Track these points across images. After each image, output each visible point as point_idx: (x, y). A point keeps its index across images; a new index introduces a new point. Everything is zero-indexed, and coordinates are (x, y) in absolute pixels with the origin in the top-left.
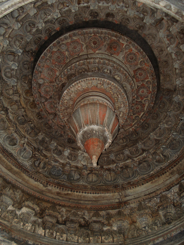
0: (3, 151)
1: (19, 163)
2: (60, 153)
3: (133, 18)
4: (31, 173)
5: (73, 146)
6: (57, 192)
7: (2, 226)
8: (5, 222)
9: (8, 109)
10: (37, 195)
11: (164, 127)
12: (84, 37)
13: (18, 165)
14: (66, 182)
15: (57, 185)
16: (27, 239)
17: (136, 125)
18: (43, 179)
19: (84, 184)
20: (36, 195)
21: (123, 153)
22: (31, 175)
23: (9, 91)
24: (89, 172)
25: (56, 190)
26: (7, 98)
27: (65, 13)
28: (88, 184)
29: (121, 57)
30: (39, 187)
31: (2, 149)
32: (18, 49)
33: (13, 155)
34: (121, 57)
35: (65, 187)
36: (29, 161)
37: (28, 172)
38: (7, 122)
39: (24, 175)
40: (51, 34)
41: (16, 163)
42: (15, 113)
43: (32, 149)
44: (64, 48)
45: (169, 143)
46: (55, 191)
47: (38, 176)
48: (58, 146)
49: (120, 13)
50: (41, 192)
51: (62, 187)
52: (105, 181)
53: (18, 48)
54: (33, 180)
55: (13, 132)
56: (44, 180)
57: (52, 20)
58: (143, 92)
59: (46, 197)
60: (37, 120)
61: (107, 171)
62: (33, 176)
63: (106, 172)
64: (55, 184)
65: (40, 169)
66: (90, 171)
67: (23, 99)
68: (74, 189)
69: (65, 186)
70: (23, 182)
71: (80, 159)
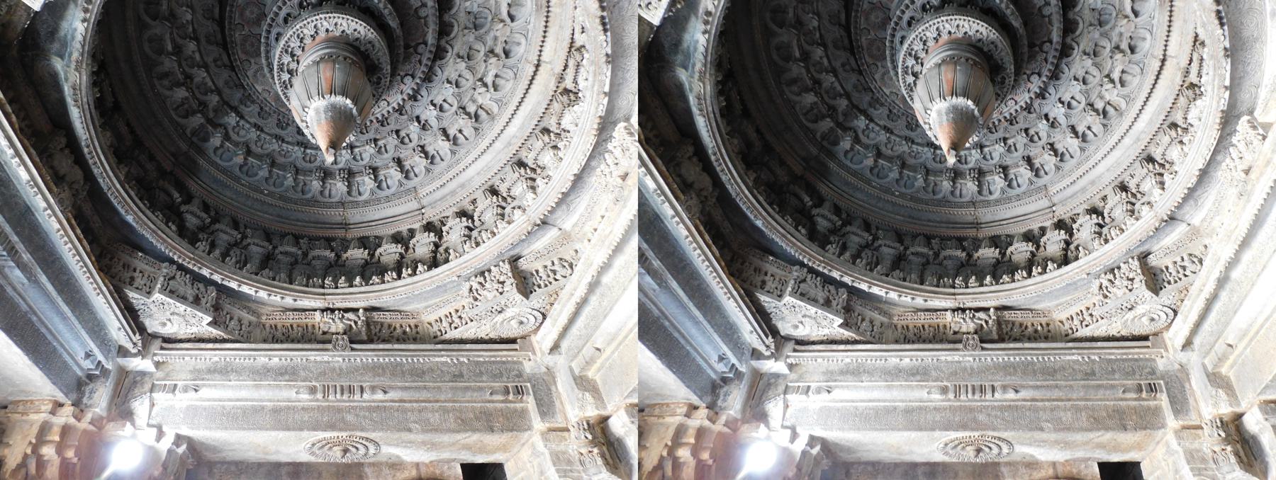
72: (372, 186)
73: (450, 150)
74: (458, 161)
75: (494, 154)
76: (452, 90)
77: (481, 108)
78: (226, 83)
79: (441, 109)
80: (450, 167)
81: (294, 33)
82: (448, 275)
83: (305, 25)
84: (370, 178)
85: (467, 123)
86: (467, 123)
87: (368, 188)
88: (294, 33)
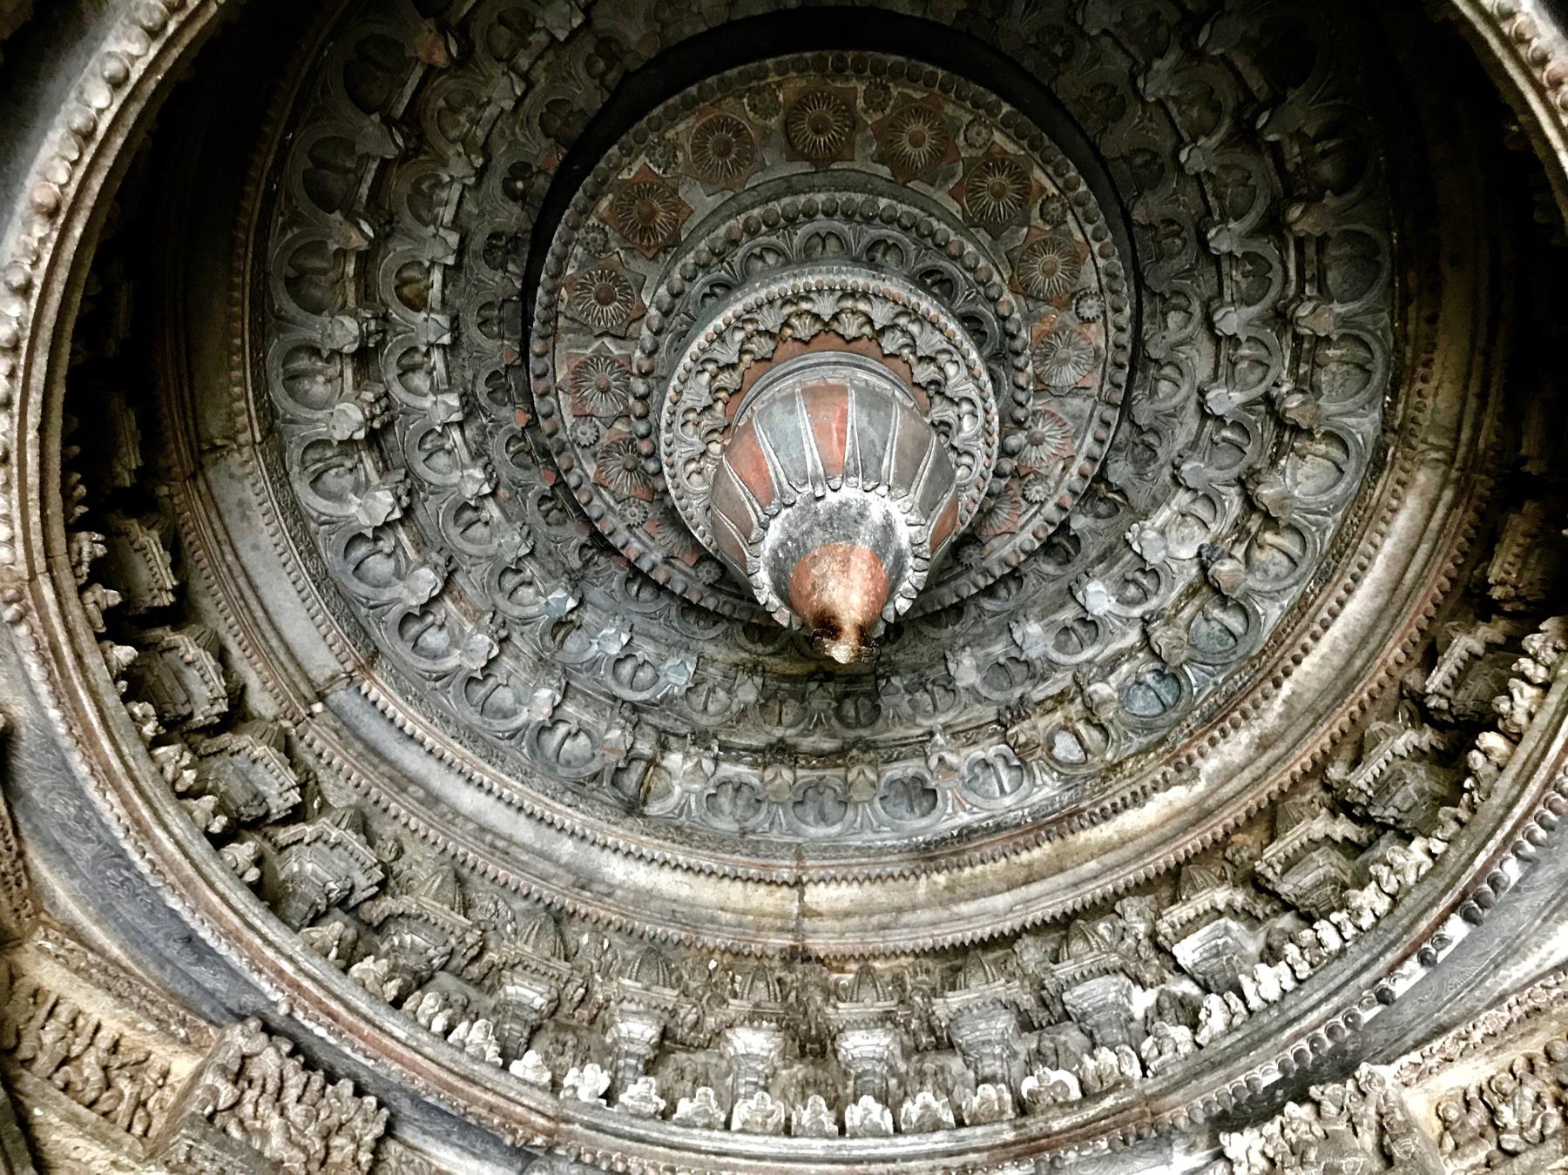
0: (924, 859)
1: (1018, 825)
2: (1090, 624)
3: (552, 82)
5: (1093, 554)
6: (1251, 742)
7: (1104, 1131)
8: (1109, 1102)
9: (781, 740)
10: (1192, 842)
12: (568, 330)
13: (1022, 834)
14: (1231, 677)
15: (1213, 727)
16: (1242, 1078)
18: (1147, 769)
19: (1285, 602)
20: (1189, 847)
21: (1234, 340)
22: (1097, 810)
24: (1239, 551)
25: (1237, 746)
26: (738, 722)
28: (1296, 583)
29: (700, 200)
30: (1178, 805)
31: (915, 854)
32: (547, 604)
33: (976, 825)
34: (700, 200)
35: (1241, 701)
36: (1039, 782)
37: (1078, 813)
38: (828, 772)
39: (1082, 836)
41: (1010, 837)
43: (995, 739)
44: (585, 433)
46: (1241, 748)
47: (1123, 784)
48: (1052, 618)
49: (514, 134)
50: (1202, 814)
51: (1233, 709)
52: (1324, 498)
53: (542, 601)
54: (1130, 812)
55: (873, 777)
56: (1154, 770)
58: (916, 142)
59: (1225, 814)
61: (1283, 462)
62: (1107, 804)
63: (1283, 472)
64: (1203, 735)
65: (1103, 752)
66: (1242, 542)
68: (1276, 665)
69: (1239, 696)
70: (1110, 859)
71: (1162, 554)
72: (364, 520)
73: (526, 725)
74: (492, 754)
75: (538, 846)
77: (647, 770)
80: (471, 736)
82: (280, 972)
85: (611, 750)
86: (611, 750)
87: (353, 509)
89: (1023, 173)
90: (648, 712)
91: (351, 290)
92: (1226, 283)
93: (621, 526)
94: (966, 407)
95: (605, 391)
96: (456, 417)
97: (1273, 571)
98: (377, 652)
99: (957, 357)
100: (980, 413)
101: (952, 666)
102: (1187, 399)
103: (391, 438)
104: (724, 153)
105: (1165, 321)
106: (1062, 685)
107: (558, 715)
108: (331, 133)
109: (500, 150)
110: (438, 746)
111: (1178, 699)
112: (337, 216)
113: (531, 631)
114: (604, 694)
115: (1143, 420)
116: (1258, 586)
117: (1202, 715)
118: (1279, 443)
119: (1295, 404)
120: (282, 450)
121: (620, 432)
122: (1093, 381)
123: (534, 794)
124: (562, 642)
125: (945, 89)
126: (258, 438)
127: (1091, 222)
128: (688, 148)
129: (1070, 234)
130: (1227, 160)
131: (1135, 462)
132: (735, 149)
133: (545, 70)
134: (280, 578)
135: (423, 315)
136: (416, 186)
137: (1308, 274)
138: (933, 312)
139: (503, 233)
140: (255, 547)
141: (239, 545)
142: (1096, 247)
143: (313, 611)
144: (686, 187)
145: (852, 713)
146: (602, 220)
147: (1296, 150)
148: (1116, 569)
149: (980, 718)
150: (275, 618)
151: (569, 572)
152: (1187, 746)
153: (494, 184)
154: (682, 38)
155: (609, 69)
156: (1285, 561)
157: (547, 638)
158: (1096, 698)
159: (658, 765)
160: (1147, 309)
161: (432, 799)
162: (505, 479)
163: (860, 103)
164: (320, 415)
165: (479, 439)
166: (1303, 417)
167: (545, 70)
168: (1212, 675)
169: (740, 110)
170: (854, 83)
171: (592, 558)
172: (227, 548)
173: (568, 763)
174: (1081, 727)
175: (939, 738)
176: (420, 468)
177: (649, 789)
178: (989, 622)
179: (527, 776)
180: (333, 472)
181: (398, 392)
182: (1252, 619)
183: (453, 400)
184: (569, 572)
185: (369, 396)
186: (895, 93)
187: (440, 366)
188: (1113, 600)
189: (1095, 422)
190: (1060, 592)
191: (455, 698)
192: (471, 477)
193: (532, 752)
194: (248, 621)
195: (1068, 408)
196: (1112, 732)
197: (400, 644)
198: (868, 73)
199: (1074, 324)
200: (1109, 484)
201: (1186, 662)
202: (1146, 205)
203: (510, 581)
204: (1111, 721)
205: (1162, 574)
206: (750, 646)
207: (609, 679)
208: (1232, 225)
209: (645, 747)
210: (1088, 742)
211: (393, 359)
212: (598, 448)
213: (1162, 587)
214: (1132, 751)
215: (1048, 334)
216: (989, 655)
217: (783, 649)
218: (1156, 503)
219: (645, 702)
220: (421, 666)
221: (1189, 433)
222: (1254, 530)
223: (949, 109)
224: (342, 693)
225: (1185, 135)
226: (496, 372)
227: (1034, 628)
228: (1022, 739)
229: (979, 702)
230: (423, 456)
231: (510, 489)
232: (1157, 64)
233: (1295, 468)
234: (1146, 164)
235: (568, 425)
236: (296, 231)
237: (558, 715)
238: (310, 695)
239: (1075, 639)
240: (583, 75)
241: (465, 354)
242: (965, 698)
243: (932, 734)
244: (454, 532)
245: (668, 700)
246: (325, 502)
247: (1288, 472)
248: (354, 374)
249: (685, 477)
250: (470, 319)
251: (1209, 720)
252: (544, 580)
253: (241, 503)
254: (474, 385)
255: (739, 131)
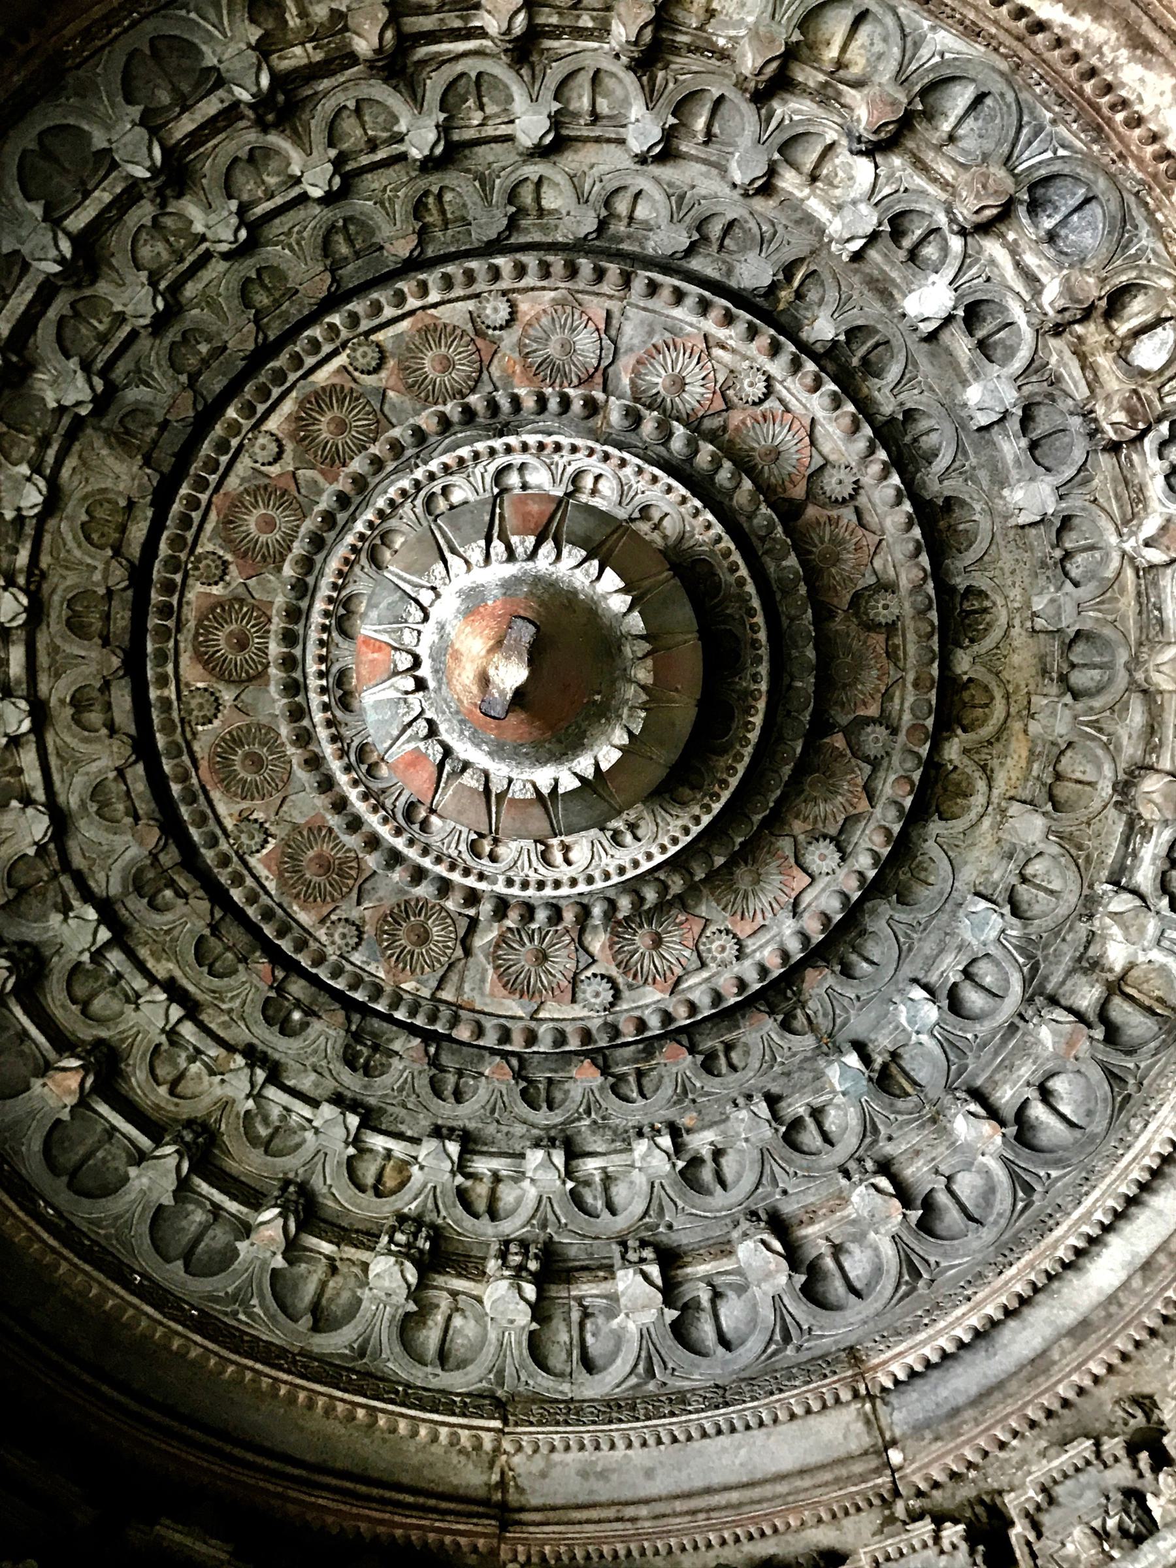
2: (973, 314)
4: (1035, 773)
11: (213, 218)
12: (459, 989)
15: (1109, 121)
17: (389, 312)
19: (926, 24)
23: (1048, 872)
27: (507, 1133)
32: (844, 1094)
40: (639, 1052)
42: (1094, 738)
43: (1135, 457)
44: (595, 993)
45: (210, 92)
46: (1150, 76)
48: (965, 366)
51: (1080, 92)
57: (594, 1132)
60: (1000, 601)
61: (721, 42)
66: (839, 93)
67: (1000, 779)
71: (864, 208)
72: (648, 1317)
73: (1006, 1162)
76: (996, 921)
78: (97, 791)
79: (955, 1005)
81: (417, 485)
83: (461, 461)
84: (646, 1277)
85: (1071, 1044)
86: (1071, 1044)
87: (632, 1327)
88: (417, 485)
89: (316, 393)
90: (1046, 978)
91: (350, 1252)
92: (489, 131)
93: (736, 968)
94: (513, 479)
95: (542, 957)
96: (559, 1158)
97: (879, 47)
98: (851, 1350)
99: (437, 487)
100: (517, 459)
101: (1023, 519)
102: (657, 180)
103: (572, 1252)
104: (257, 763)
105: (551, 212)
106: (1067, 354)
107: (1009, 1113)
108: (145, 1228)
109: (240, 1034)
110: (1003, 1300)
111: (1076, 179)
112: (242, 1246)
113: (889, 1123)
114: (1005, 1040)
115: (683, 241)
116: (893, 66)
117: (1095, 141)
118: (693, 49)
119: (622, 30)
120: (537, 1399)
121: (603, 946)
122: (597, 308)
123: (1115, 1173)
124: (915, 1083)
125: (201, 484)
126: (497, 1424)
127: (377, 308)
128: (245, 804)
129: (399, 336)
130: (318, 136)
131: (743, 249)
132: (256, 748)
133: (158, 960)
134: (700, 1453)
135: (415, 1169)
136: (253, 1140)
137: (458, 24)
138: (370, 515)
139: (347, 1047)
140: (649, 1473)
141: (642, 1494)
142: (412, 303)
143: (753, 1422)
144: (295, 813)
145: (1095, 673)
146: (322, 921)
147: (298, 50)
148: (894, 274)
149: (1114, 480)
150: (759, 1476)
151: (819, 1052)
152: (1140, 161)
153: (282, 1047)
154: (148, 793)
155: (171, 884)
156: (865, 31)
157: (900, 1104)
158: (1061, 303)
159: (1123, 978)
160: (536, 237)
161: (1081, 1330)
162: (670, 1114)
163: (217, 590)
164: (493, 1335)
165: (609, 1134)
166: (637, 16)
167: (158, 960)
168: (1038, 130)
169: (207, 736)
170: (190, 596)
171: (808, 1017)
172: (629, 1512)
173: (1089, 1113)
174: (1123, 328)
175: (1128, 546)
176: (621, 1223)
177: (1160, 1000)
178: (973, 460)
179: (1088, 1179)
180: (590, 1339)
181: (511, 1227)
182: (948, 72)
183: (536, 1157)
184: (819, 1052)
185: (492, 1265)
186: (210, 547)
187: (496, 1164)
188: (933, 277)
189: (651, 303)
190: (933, 355)
191: (945, 1255)
192: (643, 1158)
193: (1058, 1163)
194: (729, 1516)
195: (636, 341)
196: (1123, 278)
197: (847, 1313)
198: (178, 578)
199: (516, 331)
200: (773, 287)
201: (1011, 170)
202: (390, 240)
203: (810, 1137)
204: (1103, 281)
205: (898, 208)
206: (973, 815)
207: (982, 1029)
208: (402, 127)
209: (1087, 996)
210: (1148, 317)
211: (468, 1221)
212: (620, 980)
213: (918, 207)
214: (1159, 247)
215: (526, 367)
216: (1017, 461)
217: (984, 768)
218: (807, 220)
219: (1026, 982)
220: (888, 1292)
221: (706, 175)
222: (822, 78)
223: (233, 483)
224: (897, 1416)
225: (294, 192)
226: (524, 1093)
227: (973, 394)
228: (1120, 417)
229: (1086, 481)
230: (606, 1214)
231: (686, 1109)
232: (198, 228)
233: (727, 25)
234: (350, 241)
235: (585, 1013)
236: (254, 1302)
237: (1009, 1113)
238: (874, 1462)
239: (1002, 334)
240: (169, 916)
241: (491, 1129)
242: (1076, 502)
243: (1124, 554)
244: (719, 1198)
245: (1027, 947)
246: (619, 1361)
247: (732, 33)
248: (459, 1275)
249: (564, 867)
250: (448, 1112)
251: (1099, 129)
252: (818, 1091)
253: (584, 1474)
254: (533, 1126)
255: (234, 741)
